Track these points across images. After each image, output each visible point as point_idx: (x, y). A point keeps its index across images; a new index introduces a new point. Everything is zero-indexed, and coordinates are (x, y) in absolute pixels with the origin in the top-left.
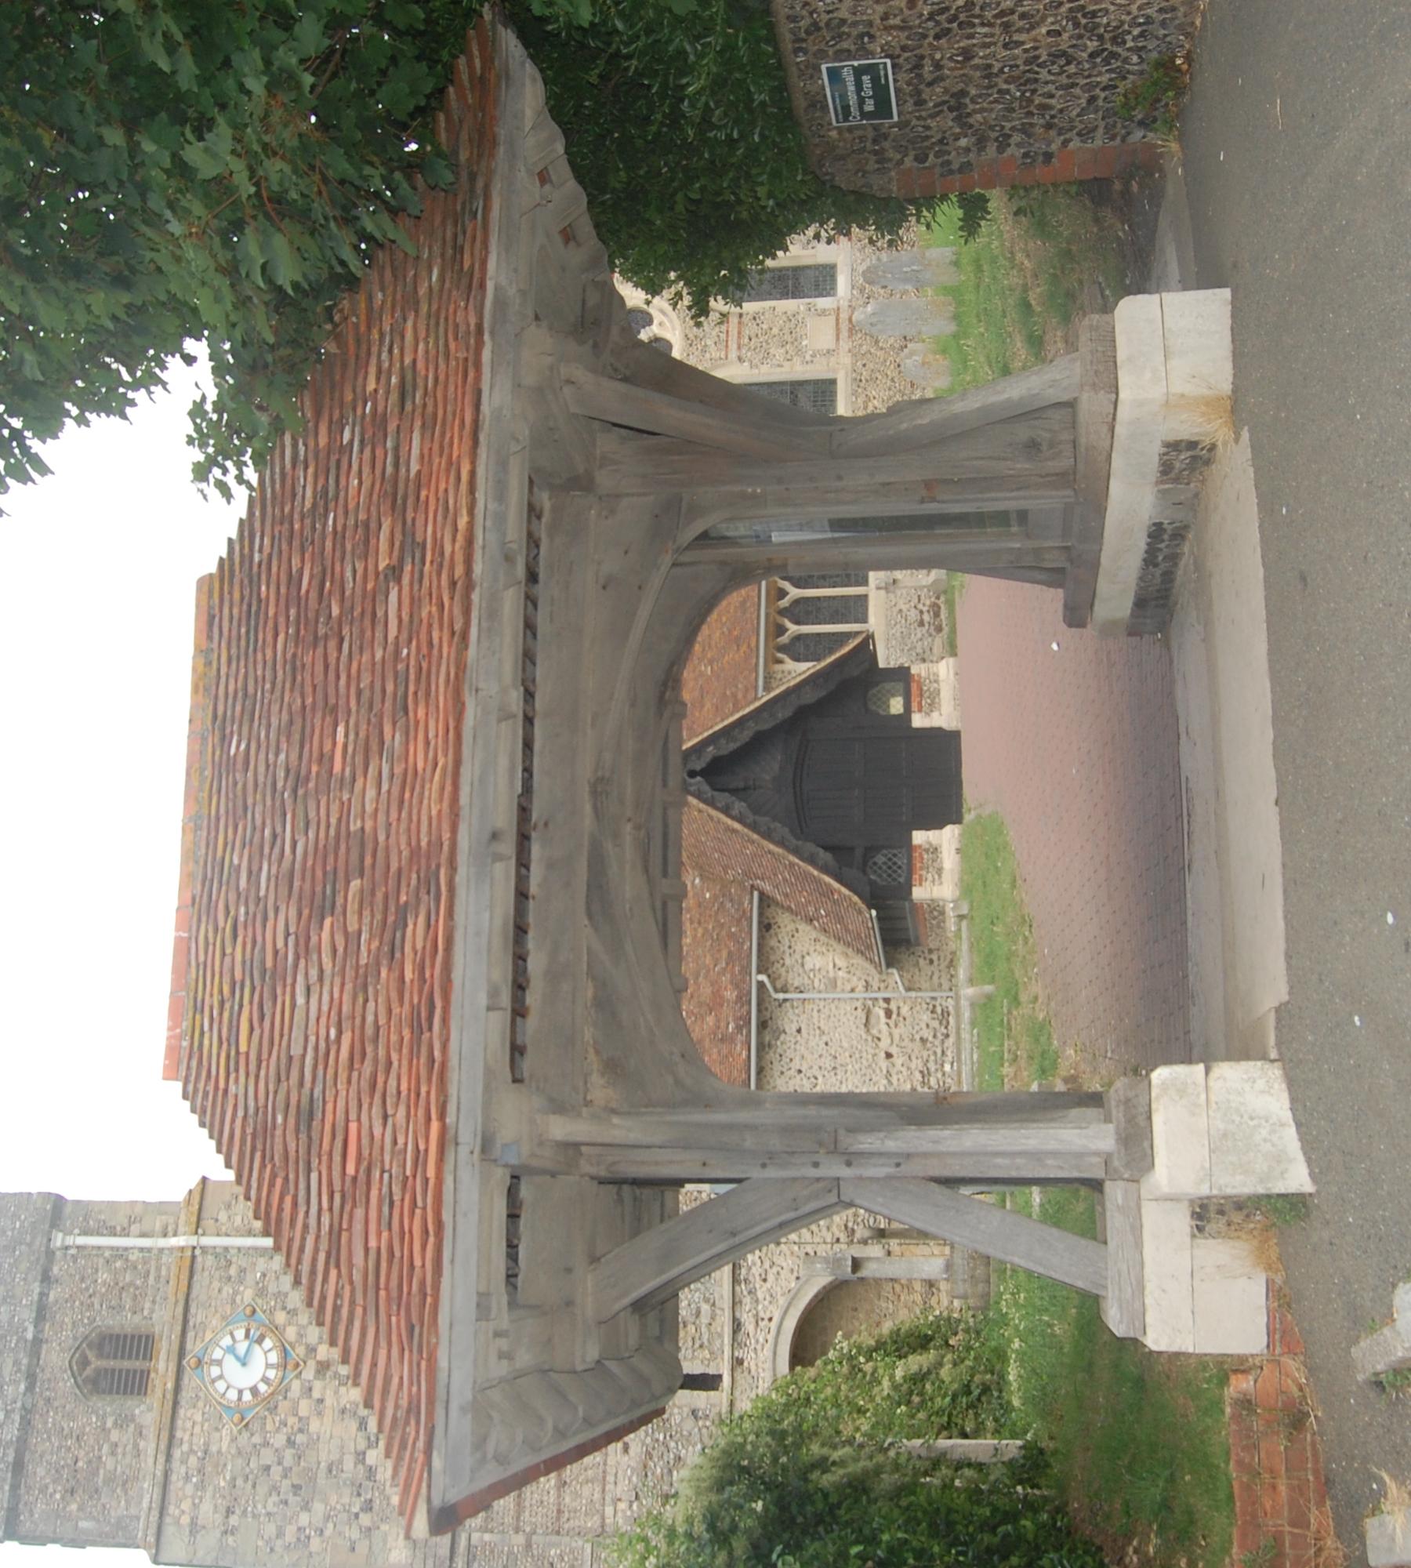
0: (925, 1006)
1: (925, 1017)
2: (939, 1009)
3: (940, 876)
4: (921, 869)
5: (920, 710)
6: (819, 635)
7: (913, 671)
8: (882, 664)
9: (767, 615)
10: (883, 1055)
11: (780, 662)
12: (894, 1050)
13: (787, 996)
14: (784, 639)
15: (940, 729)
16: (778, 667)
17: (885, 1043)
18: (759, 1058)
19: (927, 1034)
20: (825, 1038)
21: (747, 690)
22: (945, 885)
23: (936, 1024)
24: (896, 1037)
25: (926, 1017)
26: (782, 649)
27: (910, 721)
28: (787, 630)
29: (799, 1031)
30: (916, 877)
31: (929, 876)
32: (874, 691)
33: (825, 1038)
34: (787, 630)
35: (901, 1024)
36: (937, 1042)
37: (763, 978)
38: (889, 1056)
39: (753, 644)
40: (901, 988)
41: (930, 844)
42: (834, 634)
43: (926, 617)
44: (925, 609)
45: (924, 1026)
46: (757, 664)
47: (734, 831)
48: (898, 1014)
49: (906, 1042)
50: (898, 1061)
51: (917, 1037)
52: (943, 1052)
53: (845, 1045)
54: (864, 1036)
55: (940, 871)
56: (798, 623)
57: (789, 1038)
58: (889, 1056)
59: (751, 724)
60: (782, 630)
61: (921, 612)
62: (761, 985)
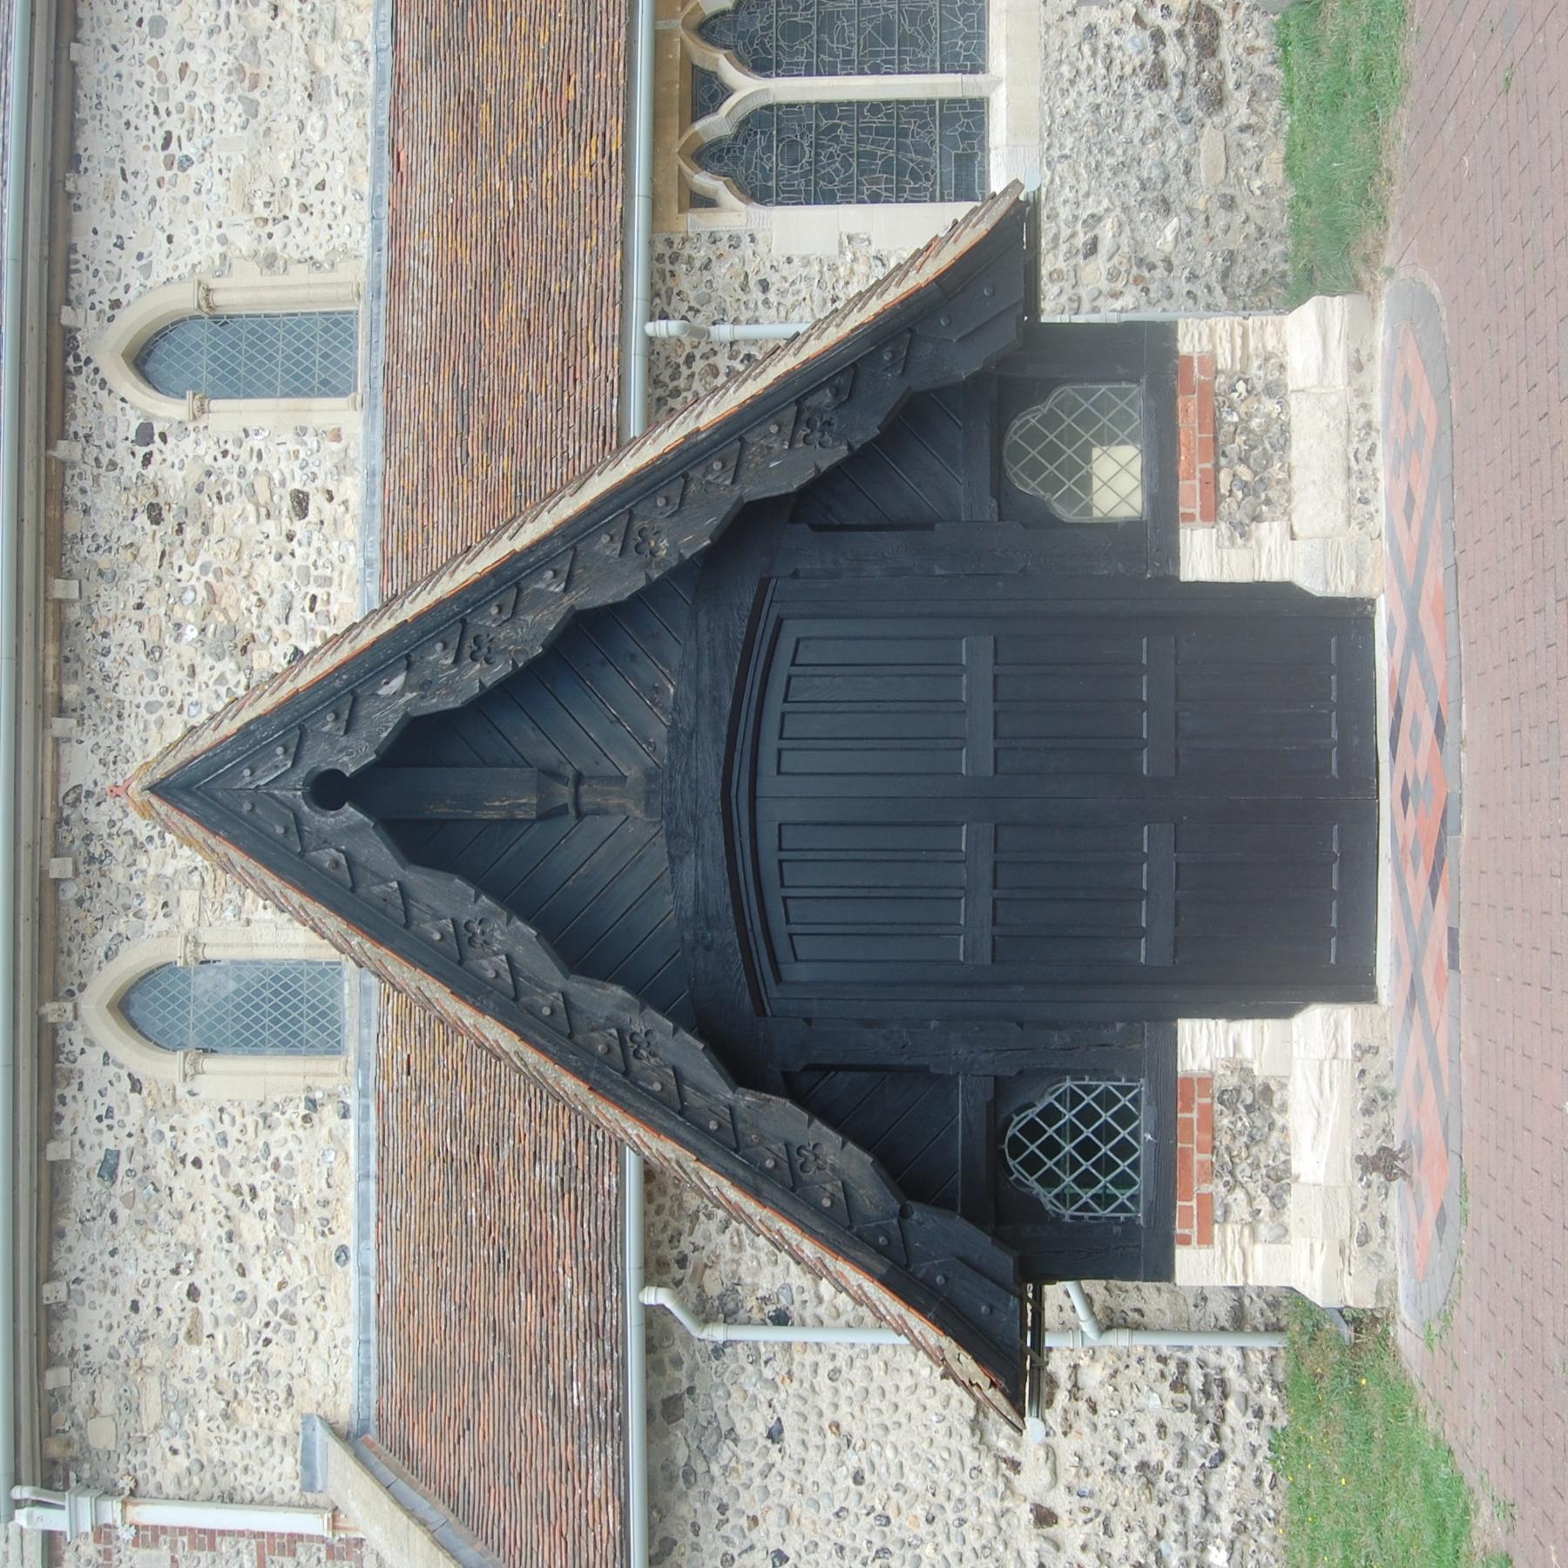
0: (1154, 1367)
1: (1154, 1402)
2: (1196, 1378)
3: (1277, 1202)
4: (1210, 1173)
5: (1211, 515)
6: (827, 108)
7: (1185, 347)
8: (1053, 309)
9: (659, 40)
10: (1026, 1516)
11: (706, 202)
12: (1059, 1502)
13: (736, 1333)
14: (717, 124)
15: (1285, 590)
16: (698, 221)
17: (1033, 1481)
18: (656, 1509)
19: (1159, 1452)
20: (853, 1460)
21: (600, 302)
22: (1298, 1245)
23: (1184, 1422)
24: (1067, 1460)
25: (1157, 1401)
26: (709, 155)
27: (1171, 553)
28: (727, 92)
29: (775, 1434)
30: (1186, 1206)
31: (1240, 1209)
32: (1031, 418)
33: (853, 1460)
34: (727, 92)
35: (1082, 1424)
36: (1188, 1477)
37: (657, 1296)
38: (1044, 1517)
39: (616, 145)
40: (1087, 1327)
41: (1246, 1072)
42: (876, 107)
43: (1173, 55)
44: (1170, 26)
45: (1150, 1431)
46: (625, 221)
47: (496, 1055)
48: (1075, 1391)
49: (1098, 1477)
50: (1072, 1533)
51: (1130, 1461)
52: (1207, 1510)
53: (914, 1481)
54: (971, 1458)
55: (1279, 1181)
56: (761, 66)
57: (750, 1451)
58: (1044, 1517)
59: (549, 584)
60: (708, 93)
61: (1158, 37)
62: (652, 1316)
